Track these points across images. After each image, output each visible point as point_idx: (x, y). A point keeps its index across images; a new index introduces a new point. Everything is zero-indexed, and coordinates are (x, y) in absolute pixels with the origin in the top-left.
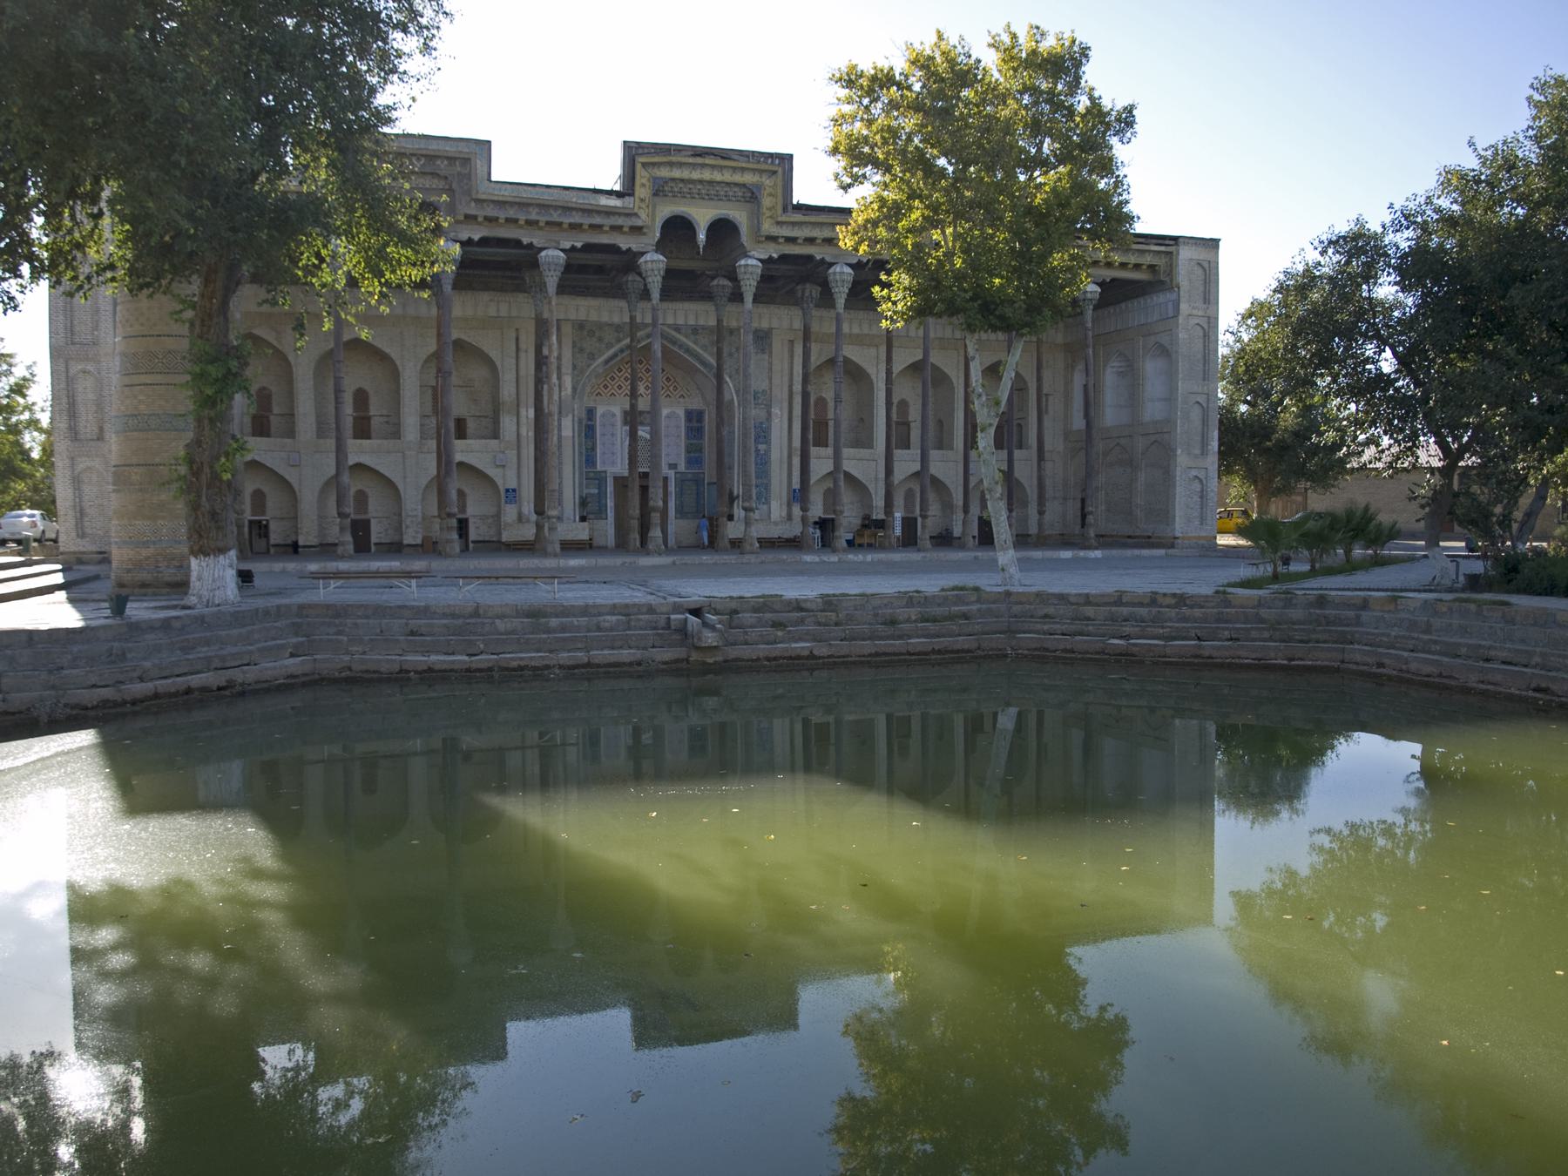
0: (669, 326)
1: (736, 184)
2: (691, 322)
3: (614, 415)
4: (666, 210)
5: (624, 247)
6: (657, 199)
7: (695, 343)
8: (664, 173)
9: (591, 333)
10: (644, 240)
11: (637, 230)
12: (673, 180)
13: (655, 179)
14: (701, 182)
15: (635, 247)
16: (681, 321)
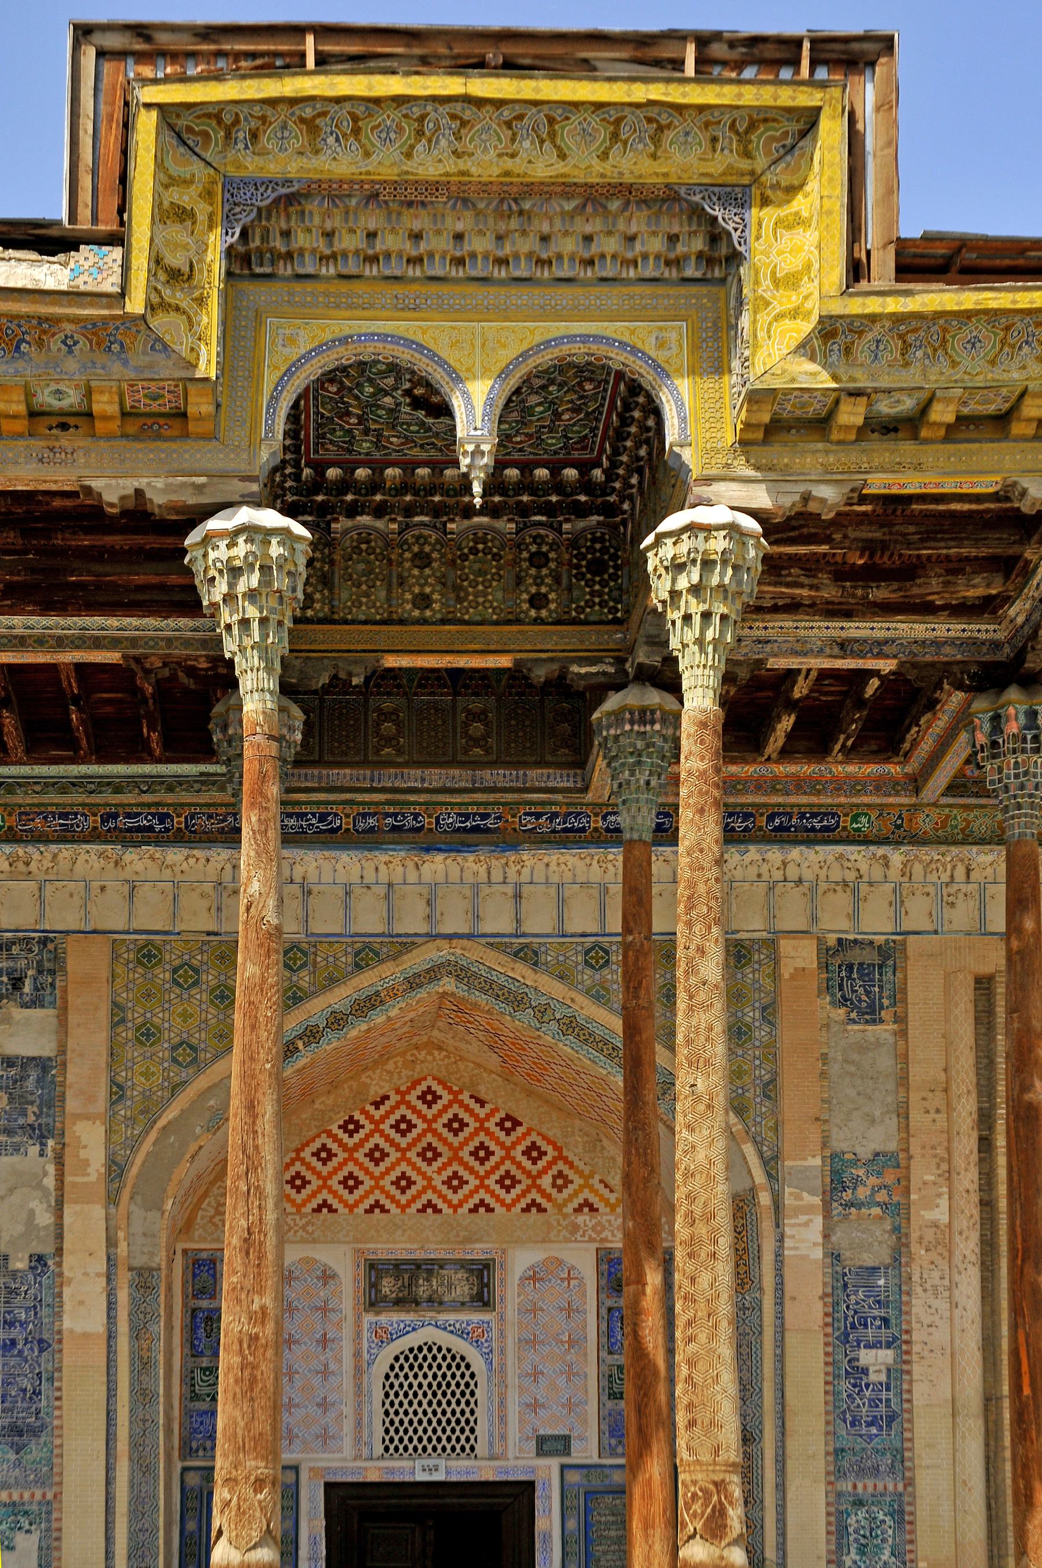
0: (496, 942)
1: (630, 194)
2: (582, 919)
3: (327, 1276)
4: (303, 342)
5: (112, 490)
6: (258, 293)
7: (599, 996)
8: (284, 161)
9: (186, 976)
10: (208, 457)
11: (163, 419)
12: (333, 192)
13: (233, 190)
14: (461, 194)
15: (161, 490)
16: (539, 921)
